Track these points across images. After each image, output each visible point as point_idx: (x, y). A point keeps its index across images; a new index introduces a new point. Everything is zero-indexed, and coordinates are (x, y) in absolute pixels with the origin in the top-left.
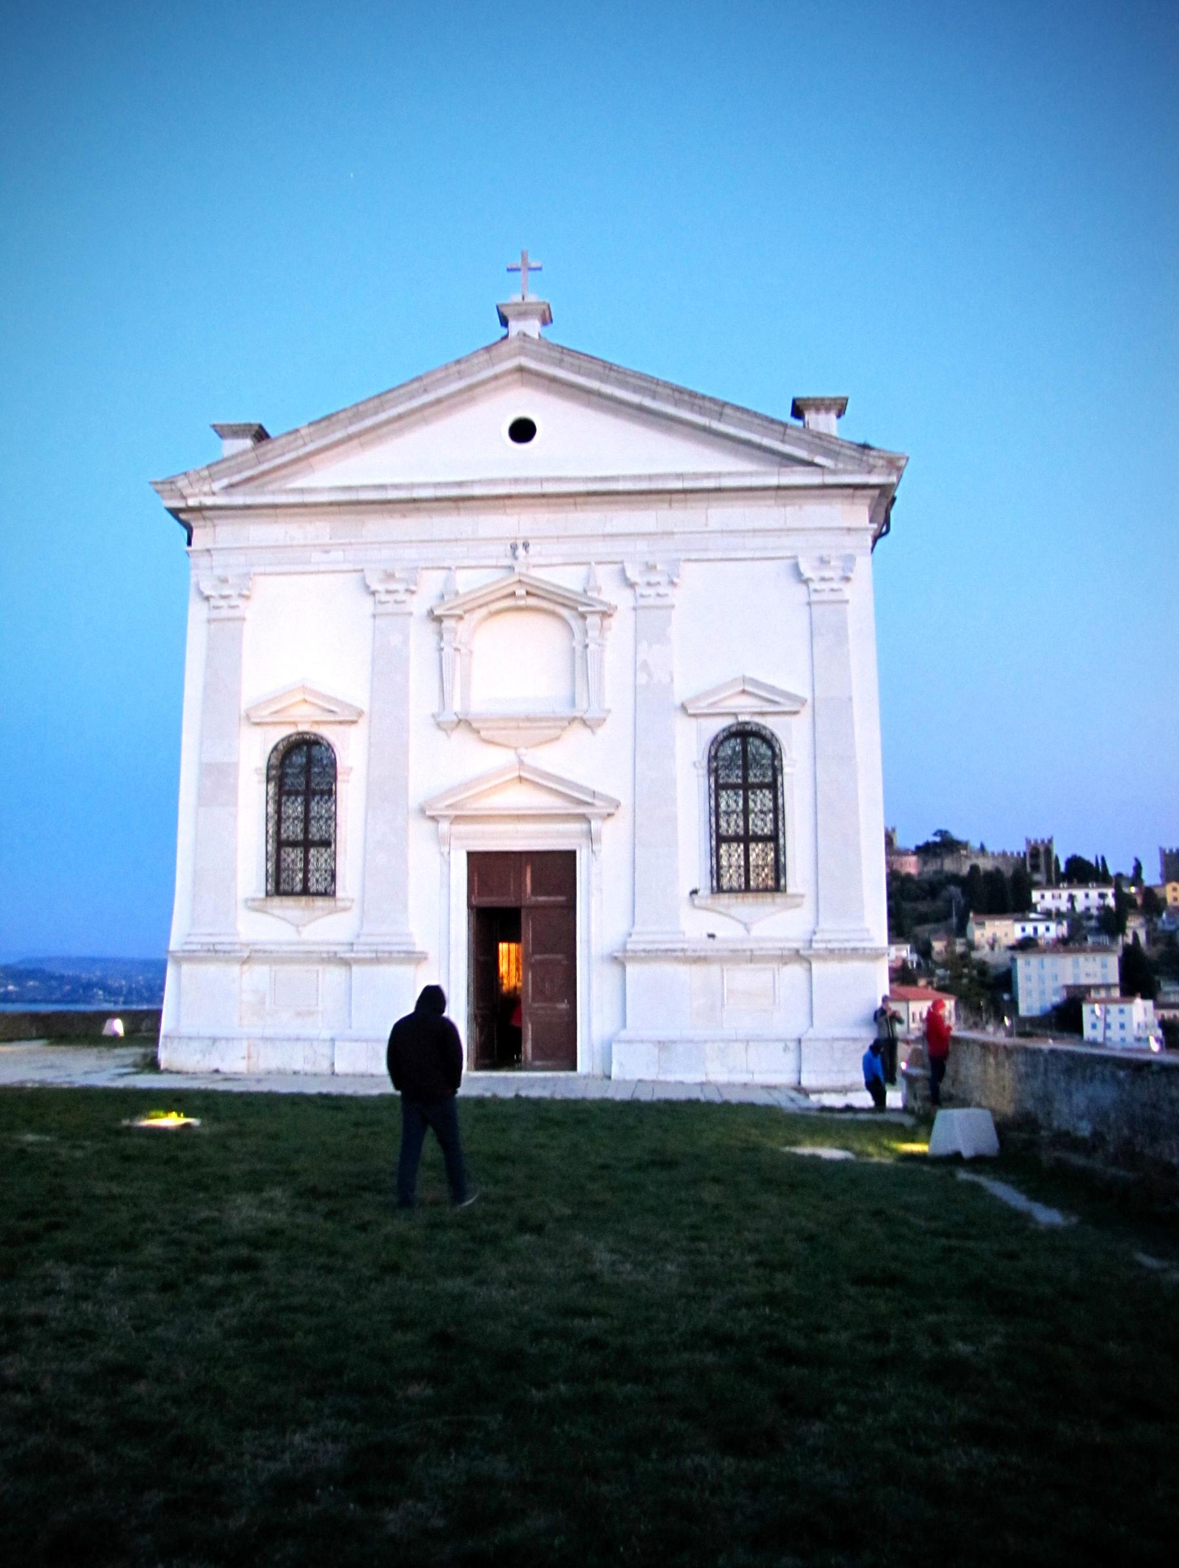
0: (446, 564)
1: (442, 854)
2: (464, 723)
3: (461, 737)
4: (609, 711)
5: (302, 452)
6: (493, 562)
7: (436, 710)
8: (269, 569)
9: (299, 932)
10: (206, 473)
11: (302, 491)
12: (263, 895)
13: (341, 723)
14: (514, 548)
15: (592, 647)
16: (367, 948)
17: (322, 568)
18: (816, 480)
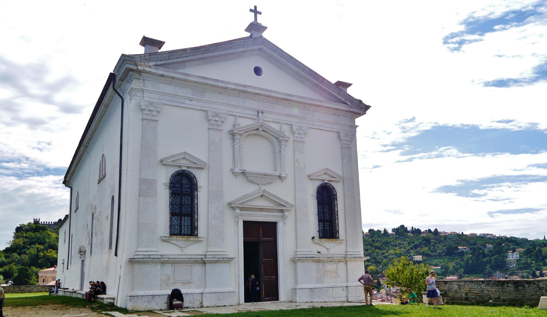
0: (235, 114)
1: (235, 221)
2: (244, 173)
3: (241, 180)
4: (287, 174)
5: (186, 59)
6: (250, 117)
7: (231, 167)
8: (168, 103)
9: (182, 250)
10: (148, 57)
11: (187, 75)
12: (168, 235)
13: (198, 168)
14: (258, 112)
15: (283, 152)
16: (212, 256)
17: (189, 106)
18: (347, 109)
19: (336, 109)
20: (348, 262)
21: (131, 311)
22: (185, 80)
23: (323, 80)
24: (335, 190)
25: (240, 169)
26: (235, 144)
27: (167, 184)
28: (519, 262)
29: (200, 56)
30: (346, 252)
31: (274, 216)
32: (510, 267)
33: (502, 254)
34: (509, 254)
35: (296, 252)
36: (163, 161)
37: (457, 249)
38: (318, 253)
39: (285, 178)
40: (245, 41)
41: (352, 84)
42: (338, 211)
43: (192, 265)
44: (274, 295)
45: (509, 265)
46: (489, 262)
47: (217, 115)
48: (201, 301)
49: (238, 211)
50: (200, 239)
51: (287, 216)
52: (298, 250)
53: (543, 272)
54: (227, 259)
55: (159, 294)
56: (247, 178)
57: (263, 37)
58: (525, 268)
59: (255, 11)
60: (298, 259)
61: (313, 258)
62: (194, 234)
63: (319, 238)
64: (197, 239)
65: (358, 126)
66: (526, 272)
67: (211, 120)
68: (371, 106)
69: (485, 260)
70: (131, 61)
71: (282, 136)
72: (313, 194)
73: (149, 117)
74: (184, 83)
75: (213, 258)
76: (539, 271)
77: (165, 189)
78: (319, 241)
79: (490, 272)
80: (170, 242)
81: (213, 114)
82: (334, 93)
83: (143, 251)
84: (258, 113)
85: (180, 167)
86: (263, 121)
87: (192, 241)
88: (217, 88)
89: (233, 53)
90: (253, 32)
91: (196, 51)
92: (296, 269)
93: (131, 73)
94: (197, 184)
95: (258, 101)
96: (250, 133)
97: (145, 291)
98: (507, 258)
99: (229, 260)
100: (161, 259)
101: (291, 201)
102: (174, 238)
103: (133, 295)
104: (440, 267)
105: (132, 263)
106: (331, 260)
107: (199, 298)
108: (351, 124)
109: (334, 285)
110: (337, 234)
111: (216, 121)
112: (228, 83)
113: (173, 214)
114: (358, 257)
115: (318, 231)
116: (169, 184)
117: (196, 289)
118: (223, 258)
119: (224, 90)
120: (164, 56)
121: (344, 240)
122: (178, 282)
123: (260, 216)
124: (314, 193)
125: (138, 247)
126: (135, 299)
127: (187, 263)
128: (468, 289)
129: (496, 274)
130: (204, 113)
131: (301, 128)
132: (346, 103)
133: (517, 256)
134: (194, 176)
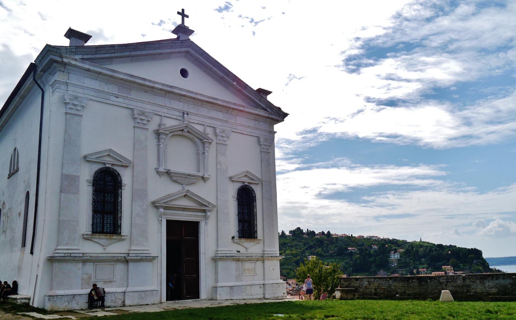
0: (161, 114)
1: (159, 220)
2: (168, 173)
4: (210, 176)
5: (113, 55)
6: (175, 117)
7: (156, 167)
8: (93, 98)
9: (105, 249)
10: (74, 50)
11: (114, 71)
12: (90, 233)
13: (122, 166)
14: (184, 113)
15: (206, 153)
16: (135, 255)
17: (115, 103)
18: (267, 115)
19: (257, 115)
20: (265, 261)
21: (50, 311)
22: (111, 76)
23: (246, 86)
24: (254, 191)
25: (164, 168)
26: (161, 143)
27: (91, 181)
28: (399, 262)
29: (127, 54)
30: (263, 251)
31: (197, 216)
32: (392, 266)
35: (217, 251)
36: (87, 157)
38: (237, 253)
39: (209, 178)
40: (173, 43)
41: (272, 92)
42: (256, 212)
43: (115, 263)
44: (195, 294)
45: (391, 264)
47: (143, 114)
48: (123, 300)
49: (162, 210)
50: (123, 238)
51: (209, 216)
52: (219, 249)
53: (419, 270)
54: (151, 258)
55: (79, 294)
56: (171, 177)
57: (190, 40)
58: (405, 267)
59: (182, 14)
60: (219, 257)
61: (234, 257)
62: (117, 232)
63: (239, 238)
64: (120, 238)
65: (276, 132)
66: (406, 270)
67: (137, 118)
68: (289, 114)
69: (371, 259)
70: (56, 52)
71: (206, 138)
72: (234, 195)
73: (73, 112)
74: (111, 79)
75: (136, 256)
76: (416, 270)
77: (88, 185)
78: (238, 241)
80: (93, 240)
81: (139, 113)
82: (255, 100)
83: (63, 249)
84: (183, 114)
85: (105, 164)
86: (188, 123)
87: (115, 239)
88: (144, 87)
89: (161, 54)
90: (180, 34)
91: (124, 47)
92: (216, 268)
93: (55, 64)
94: (121, 182)
95: (184, 102)
96: (175, 133)
97: (65, 291)
99: (151, 259)
100: (83, 258)
101: (213, 202)
102: (97, 236)
103: (53, 295)
105: (52, 261)
106: (250, 259)
107: (121, 297)
108: (271, 130)
109: (252, 283)
110: (255, 234)
111: (141, 119)
112: (155, 82)
113: (96, 211)
114: (275, 256)
115: (238, 231)
116: (92, 181)
117: (118, 288)
118: (147, 257)
119: (151, 89)
120: (91, 50)
121: (261, 240)
122: (100, 281)
123: (183, 215)
124: (234, 194)
125: (58, 245)
126: (55, 299)
127: (109, 262)
128: (377, 285)
130: (130, 110)
131: (224, 131)
132: (266, 110)
133: (398, 256)
134: (118, 173)
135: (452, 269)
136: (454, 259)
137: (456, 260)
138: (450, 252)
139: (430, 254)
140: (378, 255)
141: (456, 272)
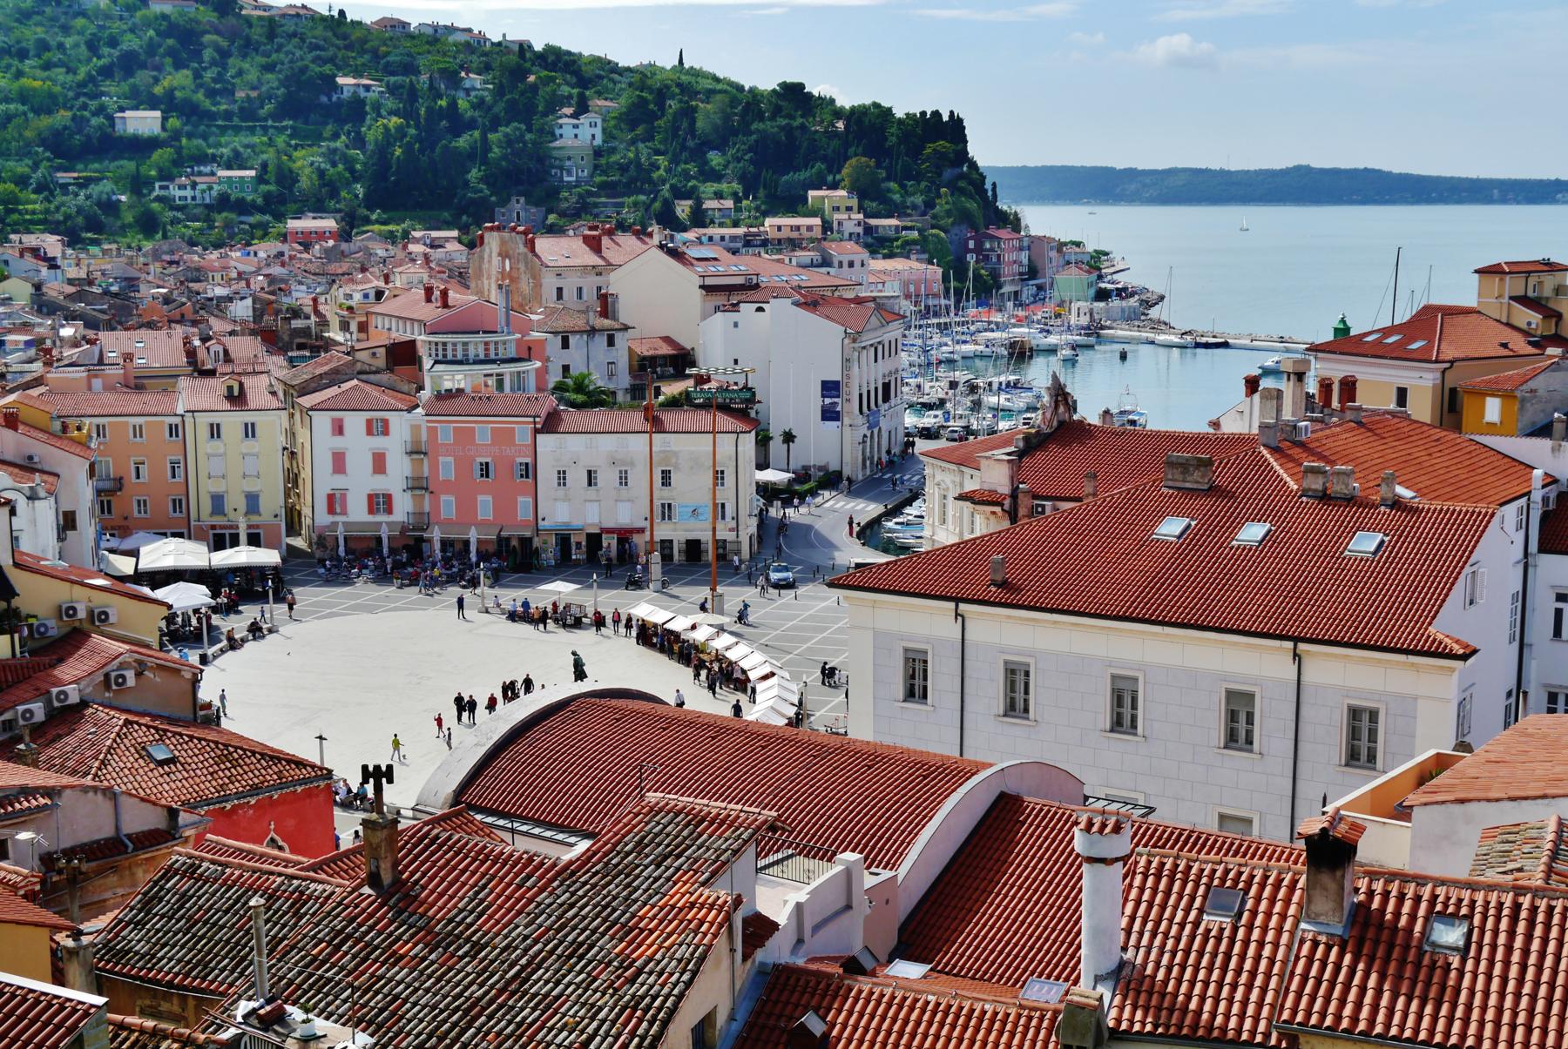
28: (603, 161)
32: (566, 179)
33: (537, 122)
34: (560, 121)
37: (330, 84)
46: (479, 154)
53: (704, 206)
58: (630, 188)
66: (635, 204)
69: (463, 142)
76: (690, 202)
79: (484, 200)
98: (554, 138)
104: (252, 173)
129: (511, 211)
133: (593, 131)
135: (856, 208)
136: (863, 159)
137: (872, 162)
138: (840, 125)
139: (754, 126)
140: (495, 125)
141: (873, 222)
